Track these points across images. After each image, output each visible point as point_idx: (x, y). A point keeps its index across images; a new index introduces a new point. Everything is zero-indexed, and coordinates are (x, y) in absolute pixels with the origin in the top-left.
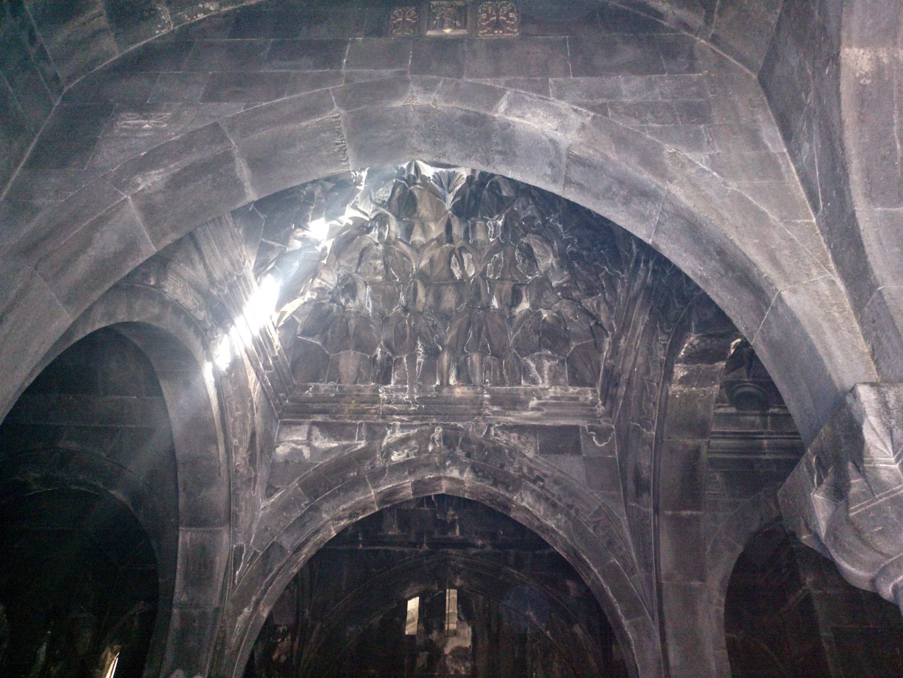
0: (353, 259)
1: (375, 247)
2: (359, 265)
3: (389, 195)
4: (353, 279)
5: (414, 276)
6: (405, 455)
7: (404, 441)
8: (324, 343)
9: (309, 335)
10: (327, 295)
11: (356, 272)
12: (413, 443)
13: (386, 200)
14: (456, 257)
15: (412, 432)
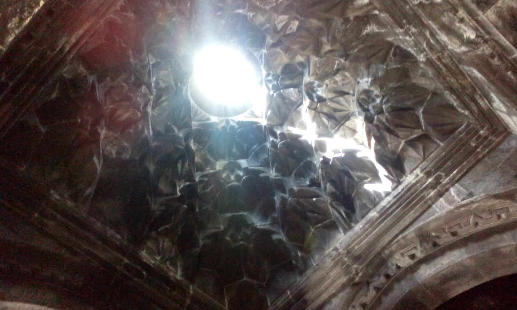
0: (347, 101)
1: (329, 86)
2: (348, 94)
3: (292, 89)
4: (360, 94)
5: (321, 57)
6: (463, 26)
7: (449, 30)
8: (420, 103)
9: (419, 121)
10: (375, 122)
11: (354, 95)
12: (445, 19)
13: (297, 90)
14: (285, 31)
15: (434, 26)
